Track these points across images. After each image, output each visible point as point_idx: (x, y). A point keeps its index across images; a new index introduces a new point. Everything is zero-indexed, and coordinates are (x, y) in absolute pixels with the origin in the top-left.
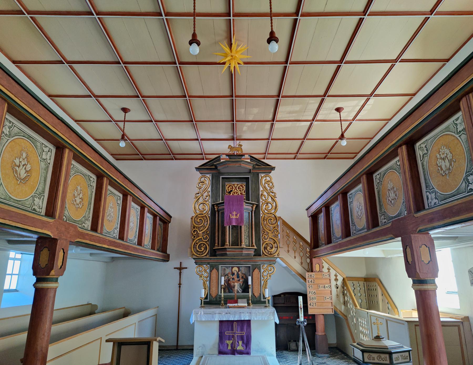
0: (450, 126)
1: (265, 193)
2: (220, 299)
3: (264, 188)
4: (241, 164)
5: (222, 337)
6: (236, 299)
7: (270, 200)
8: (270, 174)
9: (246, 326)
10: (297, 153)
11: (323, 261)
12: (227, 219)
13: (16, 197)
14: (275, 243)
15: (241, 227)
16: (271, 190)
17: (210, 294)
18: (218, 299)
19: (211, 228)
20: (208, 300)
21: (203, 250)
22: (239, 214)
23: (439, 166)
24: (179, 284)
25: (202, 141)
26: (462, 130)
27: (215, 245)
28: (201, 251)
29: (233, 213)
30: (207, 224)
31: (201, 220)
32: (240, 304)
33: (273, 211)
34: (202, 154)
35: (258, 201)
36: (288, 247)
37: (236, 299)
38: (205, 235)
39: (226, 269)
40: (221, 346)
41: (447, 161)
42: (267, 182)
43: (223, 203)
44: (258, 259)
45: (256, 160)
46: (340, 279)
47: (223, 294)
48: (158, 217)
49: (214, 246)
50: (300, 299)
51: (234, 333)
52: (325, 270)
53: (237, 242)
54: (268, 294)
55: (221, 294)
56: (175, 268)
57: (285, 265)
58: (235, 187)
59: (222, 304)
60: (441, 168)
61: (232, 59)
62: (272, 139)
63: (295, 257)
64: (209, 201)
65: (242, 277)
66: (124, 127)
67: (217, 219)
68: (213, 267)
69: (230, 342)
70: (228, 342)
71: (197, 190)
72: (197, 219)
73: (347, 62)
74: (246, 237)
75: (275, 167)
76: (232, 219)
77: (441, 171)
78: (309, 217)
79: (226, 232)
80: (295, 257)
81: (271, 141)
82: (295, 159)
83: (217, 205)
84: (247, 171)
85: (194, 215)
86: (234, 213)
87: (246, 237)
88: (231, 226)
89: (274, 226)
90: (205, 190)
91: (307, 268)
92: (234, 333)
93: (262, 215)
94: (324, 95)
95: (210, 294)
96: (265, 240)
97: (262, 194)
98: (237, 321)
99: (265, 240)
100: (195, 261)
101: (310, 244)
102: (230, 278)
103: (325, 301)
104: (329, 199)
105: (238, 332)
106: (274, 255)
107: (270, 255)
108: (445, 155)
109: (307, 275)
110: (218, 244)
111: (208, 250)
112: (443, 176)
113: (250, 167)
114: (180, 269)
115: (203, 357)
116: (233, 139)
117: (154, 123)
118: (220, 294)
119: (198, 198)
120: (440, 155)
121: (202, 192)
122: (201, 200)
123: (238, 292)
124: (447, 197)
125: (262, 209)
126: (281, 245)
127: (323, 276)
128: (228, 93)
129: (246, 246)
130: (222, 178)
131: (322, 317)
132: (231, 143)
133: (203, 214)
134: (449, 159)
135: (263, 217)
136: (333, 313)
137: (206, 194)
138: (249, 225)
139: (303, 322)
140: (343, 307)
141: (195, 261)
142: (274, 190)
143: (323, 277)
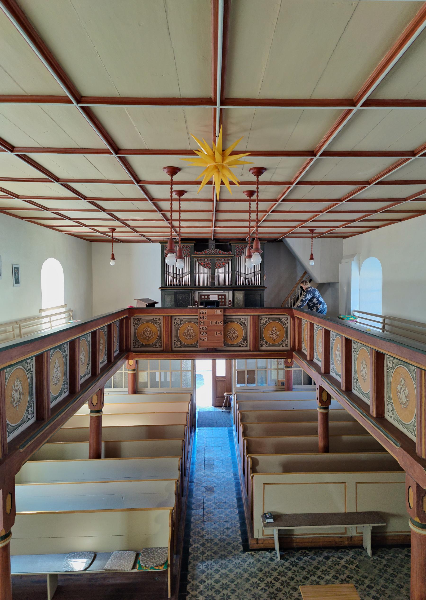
13: (403, 420)
41: (18, 393)
112: (14, 407)
120: (15, 386)
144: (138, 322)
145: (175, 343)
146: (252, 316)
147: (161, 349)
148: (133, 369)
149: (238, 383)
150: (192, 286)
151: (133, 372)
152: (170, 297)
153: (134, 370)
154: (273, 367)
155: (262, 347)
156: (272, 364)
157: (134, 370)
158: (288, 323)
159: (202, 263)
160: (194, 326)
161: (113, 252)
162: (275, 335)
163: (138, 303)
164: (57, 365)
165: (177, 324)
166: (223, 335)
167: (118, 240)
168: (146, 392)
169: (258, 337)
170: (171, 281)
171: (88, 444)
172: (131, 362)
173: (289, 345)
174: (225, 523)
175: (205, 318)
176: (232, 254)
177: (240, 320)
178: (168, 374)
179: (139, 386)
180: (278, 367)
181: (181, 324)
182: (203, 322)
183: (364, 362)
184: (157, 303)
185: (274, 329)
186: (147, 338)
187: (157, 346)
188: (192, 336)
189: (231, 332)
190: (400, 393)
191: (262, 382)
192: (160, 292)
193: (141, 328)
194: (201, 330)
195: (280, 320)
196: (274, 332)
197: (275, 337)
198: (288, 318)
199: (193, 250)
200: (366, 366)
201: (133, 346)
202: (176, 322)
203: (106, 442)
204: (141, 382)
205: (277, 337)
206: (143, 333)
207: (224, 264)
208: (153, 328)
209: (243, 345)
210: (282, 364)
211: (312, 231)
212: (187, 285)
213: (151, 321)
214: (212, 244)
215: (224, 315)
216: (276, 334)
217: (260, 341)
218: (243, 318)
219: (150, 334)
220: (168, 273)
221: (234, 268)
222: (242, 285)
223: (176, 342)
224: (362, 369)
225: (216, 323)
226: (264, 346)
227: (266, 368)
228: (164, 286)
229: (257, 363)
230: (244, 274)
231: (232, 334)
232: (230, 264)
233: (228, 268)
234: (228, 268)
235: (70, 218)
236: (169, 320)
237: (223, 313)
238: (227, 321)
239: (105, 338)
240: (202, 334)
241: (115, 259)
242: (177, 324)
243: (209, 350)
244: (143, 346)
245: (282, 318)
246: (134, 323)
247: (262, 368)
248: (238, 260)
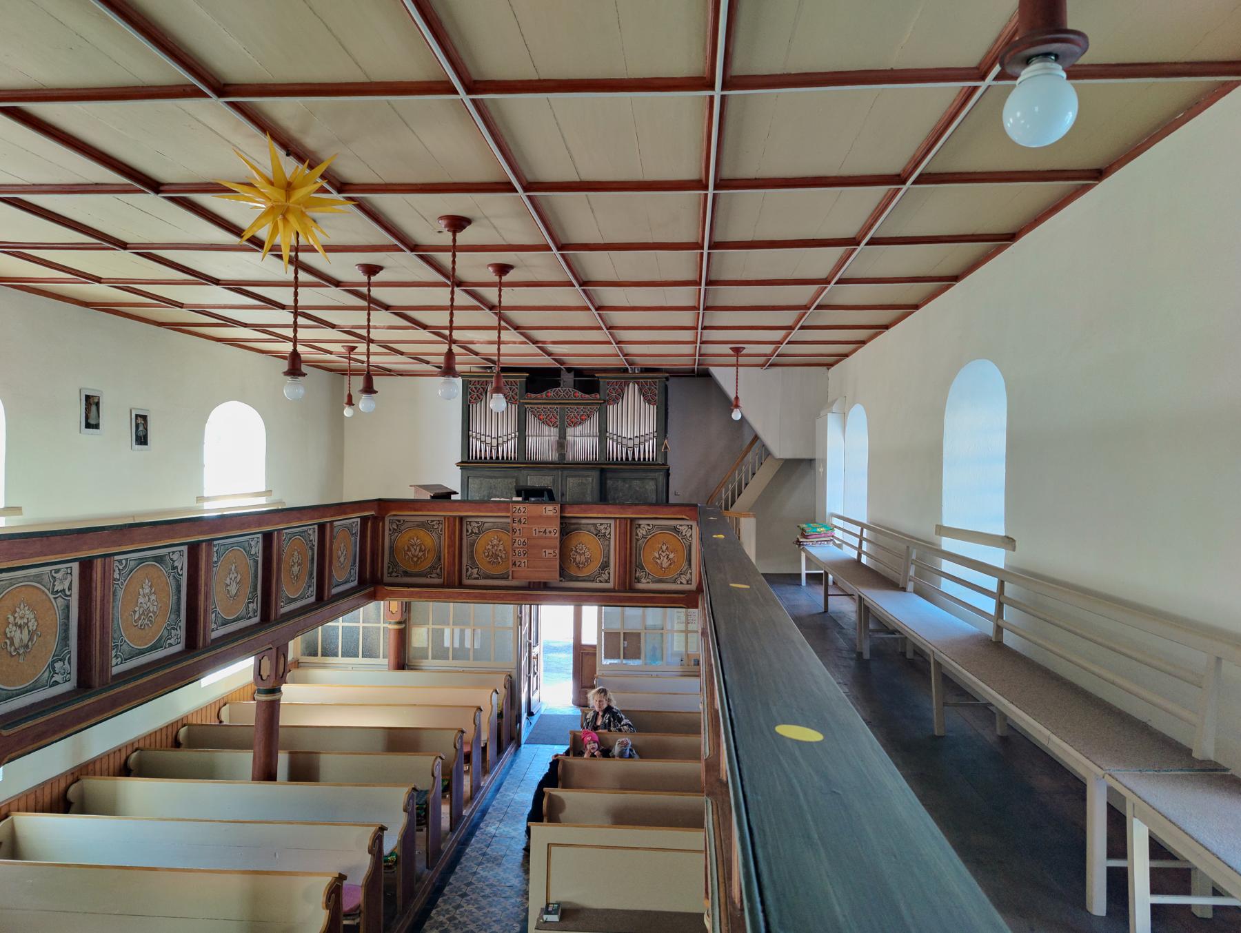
0: (43, 577)
23: (8, 638)
26: (61, 591)
60: (11, 643)
77: (11, 647)
108: (26, 621)
124: (13, 694)
134: (30, 629)
144: (397, 527)
145: (467, 570)
146: (618, 520)
147: (439, 581)
148: (398, 620)
149: (605, 658)
150: (520, 461)
151: (396, 627)
152: (477, 481)
153: (399, 623)
154: (676, 627)
155: (639, 582)
156: (676, 622)
157: (399, 623)
158: (691, 535)
159: (540, 415)
160: (505, 537)
161: (350, 391)
162: (665, 560)
163: (416, 492)
165: (472, 532)
166: (558, 556)
167: (390, 370)
168: (423, 668)
169: (631, 562)
170: (481, 451)
171: (252, 755)
172: (395, 605)
173: (694, 580)
174: (493, 923)
175: (523, 521)
176: (600, 400)
177: (596, 529)
178: (468, 632)
179: (411, 653)
180: (687, 627)
181: (479, 533)
182: (520, 530)
184: (455, 493)
185: (664, 548)
186: (415, 559)
187: (432, 576)
188: (501, 557)
189: (577, 552)
191: (654, 658)
192: (458, 471)
193: (404, 540)
194: (516, 545)
195: (675, 529)
196: (664, 554)
197: (665, 564)
198: (692, 526)
199: (524, 390)
201: (388, 573)
202: (470, 528)
203: (293, 755)
204: (415, 648)
205: (670, 564)
206: (406, 548)
207: (583, 417)
208: (428, 540)
209: (600, 579)
210: (696, 622)
211: (737, 351)
212: (511, 458)
213: (423, 525)
214: (568, 378)
215: (562, 518)
216: (667, 558)
217: (636, 570)
218: (601, 524)
219: (421, 550)
220: (474, 434)
221: (604, 426)
222: (619, 459)
223: (470, 569)
225: (545, 532)
226: (643, 580)
227: (663, 629)
228: (466, 459)
229: (644, 616)
230: (625, 438)
231: (580, 554)
232: (596, 416)
233: (592, 426)
234: (592, 426)
235: (246, 324)
236: (455, 524)
237: (558, 514)
238: (567, 529)
239: (310, 553)
240: (517, 553)
241: (353, 405)
242: (472, 532)
243: (531, 586)
244: (406, 574)
245: (681, 525)
246: (390, 530)
247: (654, 628)
248: (612, 410)
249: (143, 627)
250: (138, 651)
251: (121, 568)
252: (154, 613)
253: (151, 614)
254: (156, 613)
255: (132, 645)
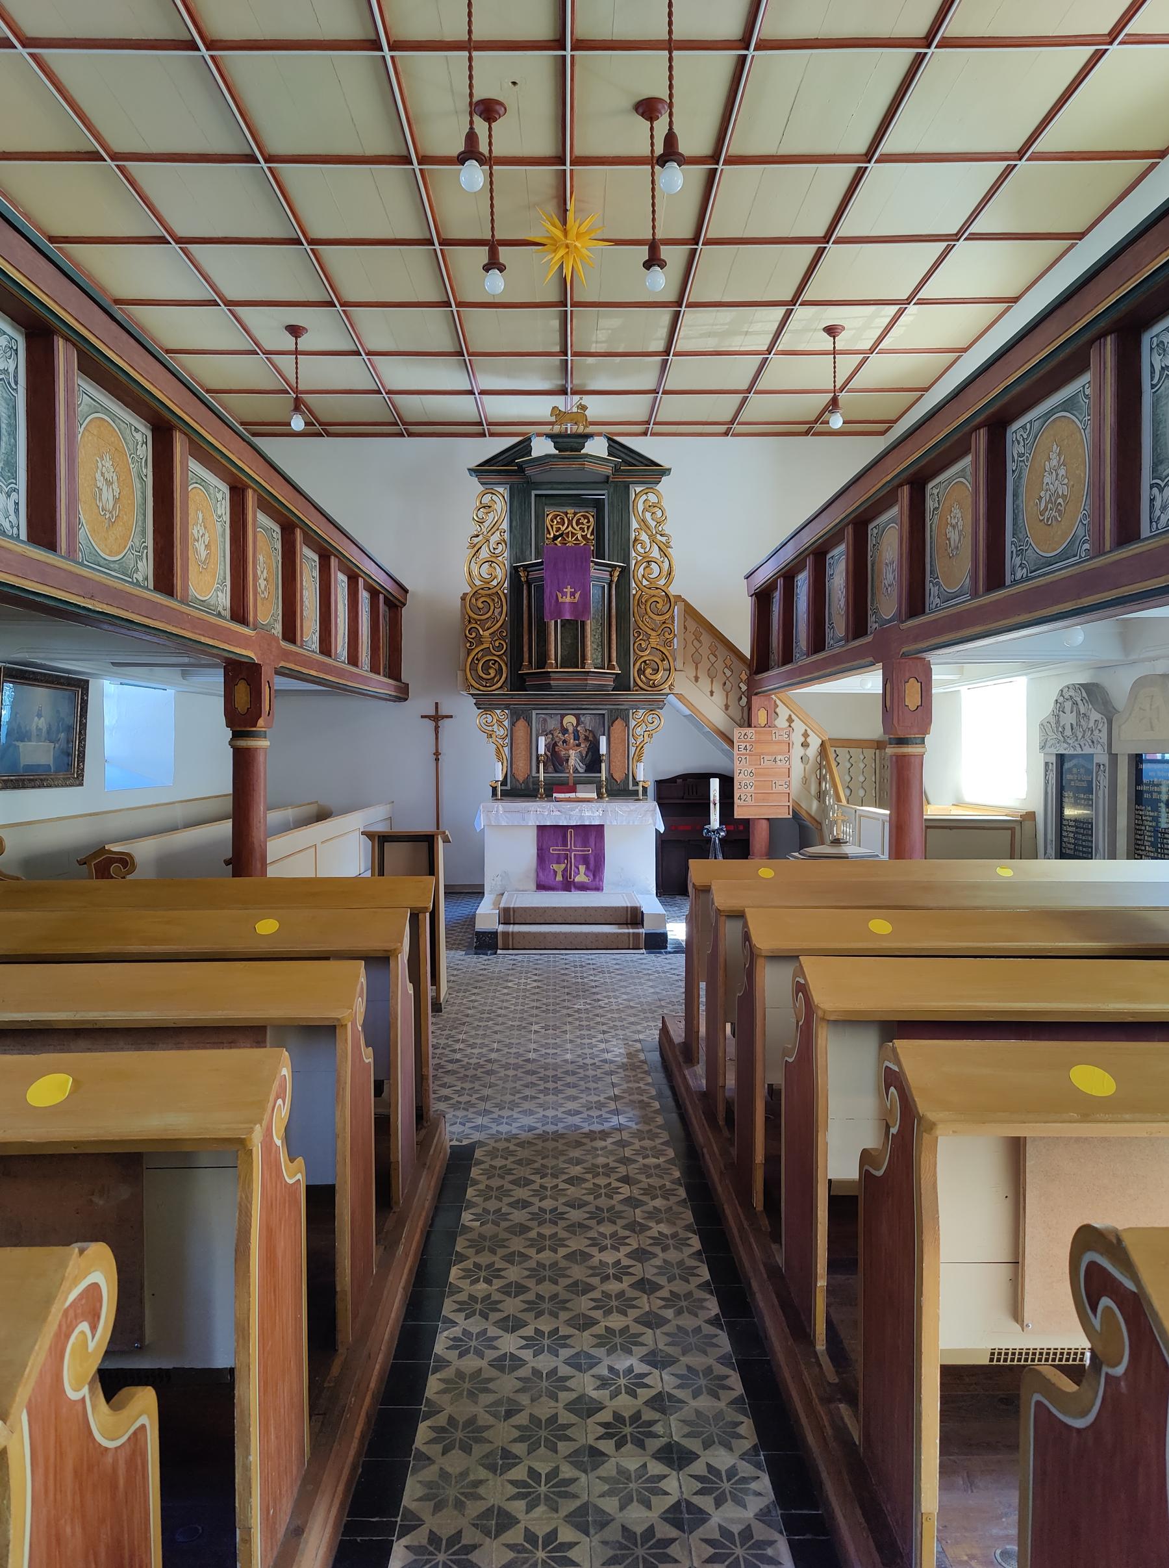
1: (644, 537)
2: (535, 787)
3: (642, 523)
4: (584, 464)
5: (543, 857)
6: (571, 783)
7: (655, 553)
8: (658, 487)
9: (593, 837)
10: (732, 422)
11: (778, 702)
12: (551, 605)
14: (664, 660)
15: (583, 624)
16: (660, 529)
17: (513, 775)
18: (531, 786)
19: (512, 621)
20: (508, 787)
21: (492, 675)
22: (579, 593)
24: (434, 754)
25: (484, 397)
27: (521, 665)
28: (489, 677)
29: (565, 590)
30: (501, 613)
31: (485, 603)
32: (580, 795)
33: (662, 582)
34: (480, 424)
35: (626, 558)
36: (697, 669)
37: (571, 783)
38: (496, 640)
39: (548, 718)
40: (541, 874)
42: (650, 506)
43: (541, 564)
44: (623, 696)
45: (623, 450)
46: (815, 742)
47: (542, 776)
48: (381, 596)
49: (520, 667)
50: (715, 784)
51: (566, 850)
52: (781, 722)
53: (574, 657)
54: (645, 773)
55: (537, 775)
56: (422, 717)
57: (688, 712)
58: (568, 519)
59: (542, 795)
61: (567, 253)
62: (665, 392)
63: (712, 693)
64: (505, 555)
65: (586, 739)
66: (297, 378)
67: (525, 602)
68: (515, 716)
69: (559, 868)
70: (555, 866)
71: (474, 529)
72: (476, 600)
73: (841, 241)
74: (595, 647)
75: (669, 470)
76: (564, 603)
78: (751, 596)
79: (549, 634)
80: (712, 693)
81: (661, 397)
82: (728, 435)
83: (526, 567)
84: (602, 479)
85: (468, 590)
86: (568, 590)
87: (595, 647)
88: (559, 621)
89: (662, 618)
90: (494, 527)
91: (738, 718)
92: (566, 850)
93: (634, 592)
94: (793, 302)
95: (513, 775)
96: (641, 654)
97: (636, 540)
98: (575, 827)
99: (641, 654)
100: (474, 701)
101: (748, 663)
102: (557, 739)
103: (774, 790)
104: (788, 564)
105: (575, 849)
106: (662, 687)
107: (651, 687)
109: (737, 733)
110: (530, 662)
111: (504, 676)
113: (608, 470)
114: (437, 718)
115: (506, 893)
116: (563, 392)
117: (366, 358)
118: (534, 774)
119: (476, 549)
121: (485, 533)
122: (484, 554)
123: (576, 771)
125: (636, 577)
126: (679, 665)
127: (774, 735)
128: (554, 297)
129: (595, 668)
130: (536, 495)
131: (765, 824)
132: (559, 401)
133: (490, 589)
135: (637, 597)
136: (790, 816)
137: (496, 537)
138: (602, 617)
139: (718, 831)
140: (815, 804)
141: (474, 701)
142: (667, 528)
143: (774, 739)
164: (1054, 463)
183: (108, 464)
190: (198, 541)
200: (115, 478)
224: (101, 483)
249: (1049, 523)
250: (1044, 560)
251: (1025, 437)
252: (1064, 497)
253: (1060, 500)
254: (1066, 496)
255: (1038, 551)
